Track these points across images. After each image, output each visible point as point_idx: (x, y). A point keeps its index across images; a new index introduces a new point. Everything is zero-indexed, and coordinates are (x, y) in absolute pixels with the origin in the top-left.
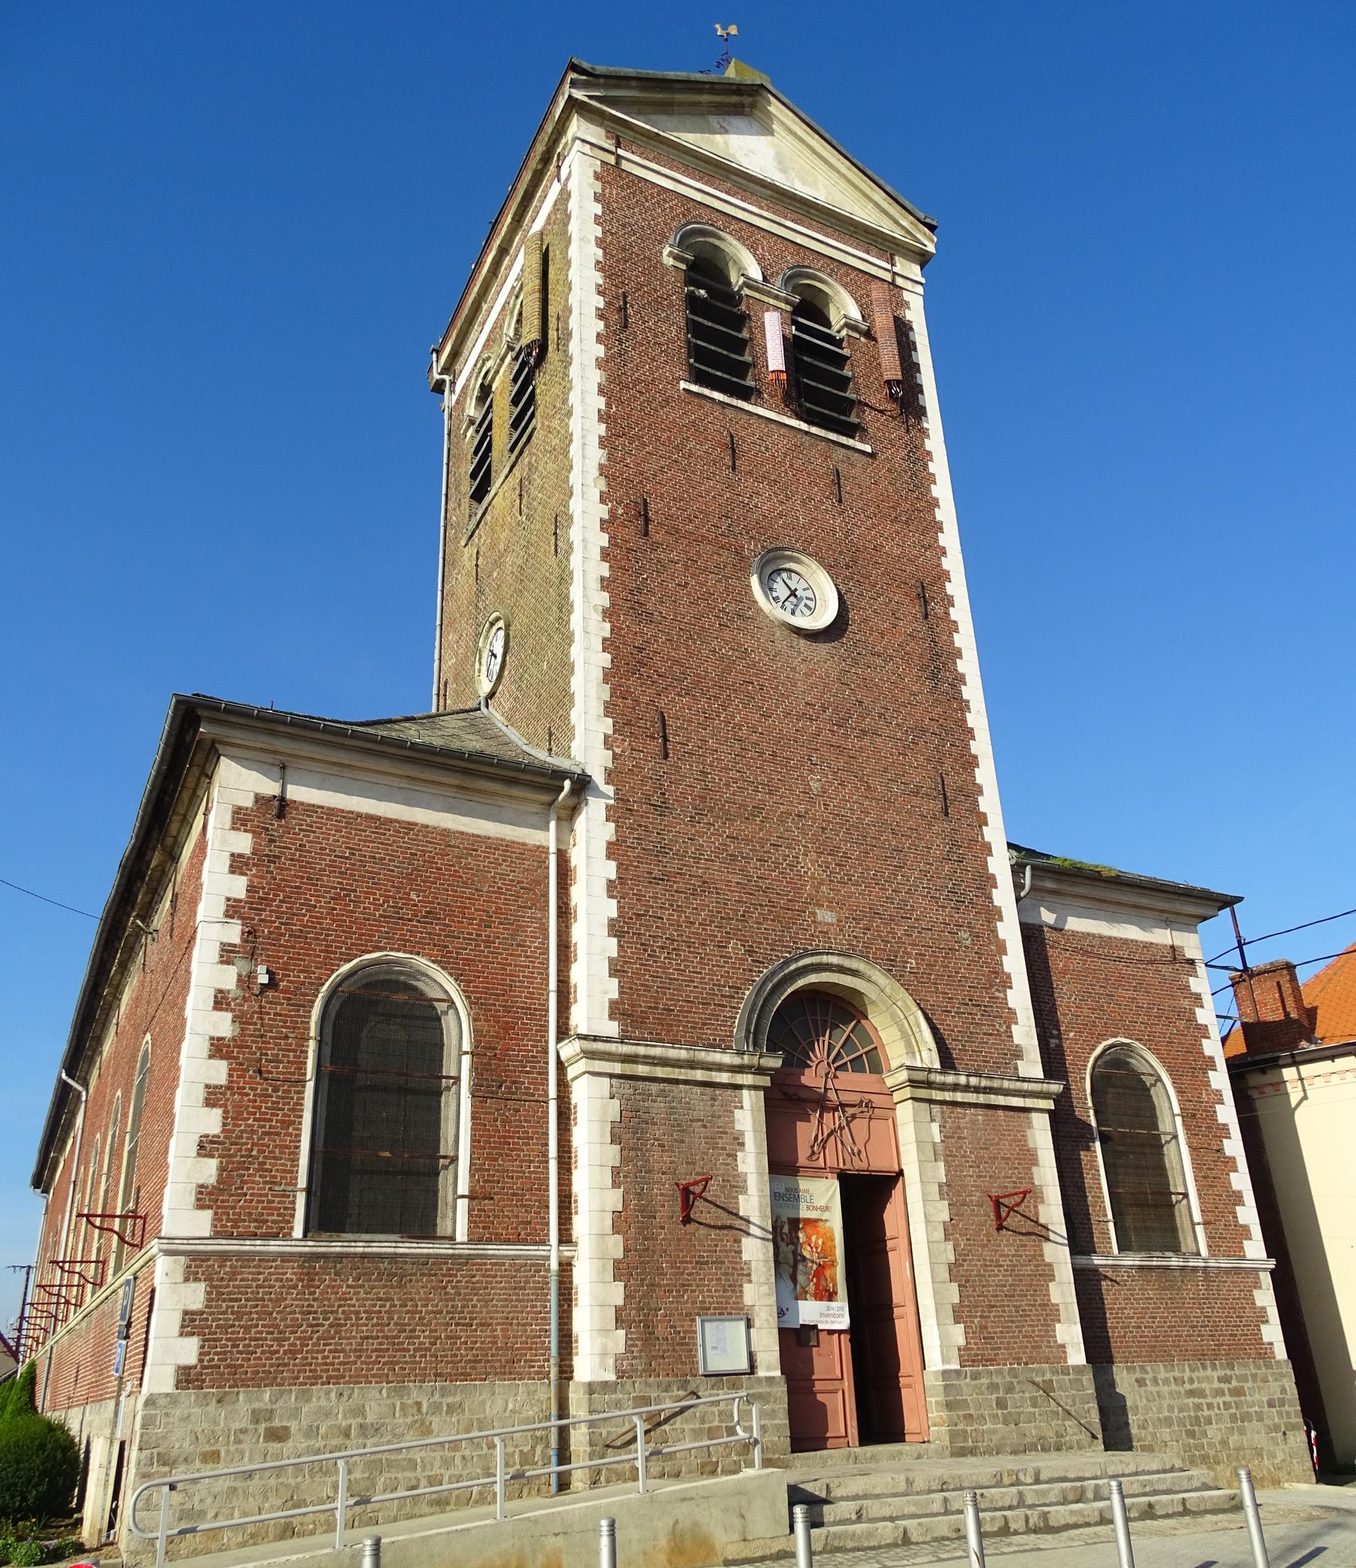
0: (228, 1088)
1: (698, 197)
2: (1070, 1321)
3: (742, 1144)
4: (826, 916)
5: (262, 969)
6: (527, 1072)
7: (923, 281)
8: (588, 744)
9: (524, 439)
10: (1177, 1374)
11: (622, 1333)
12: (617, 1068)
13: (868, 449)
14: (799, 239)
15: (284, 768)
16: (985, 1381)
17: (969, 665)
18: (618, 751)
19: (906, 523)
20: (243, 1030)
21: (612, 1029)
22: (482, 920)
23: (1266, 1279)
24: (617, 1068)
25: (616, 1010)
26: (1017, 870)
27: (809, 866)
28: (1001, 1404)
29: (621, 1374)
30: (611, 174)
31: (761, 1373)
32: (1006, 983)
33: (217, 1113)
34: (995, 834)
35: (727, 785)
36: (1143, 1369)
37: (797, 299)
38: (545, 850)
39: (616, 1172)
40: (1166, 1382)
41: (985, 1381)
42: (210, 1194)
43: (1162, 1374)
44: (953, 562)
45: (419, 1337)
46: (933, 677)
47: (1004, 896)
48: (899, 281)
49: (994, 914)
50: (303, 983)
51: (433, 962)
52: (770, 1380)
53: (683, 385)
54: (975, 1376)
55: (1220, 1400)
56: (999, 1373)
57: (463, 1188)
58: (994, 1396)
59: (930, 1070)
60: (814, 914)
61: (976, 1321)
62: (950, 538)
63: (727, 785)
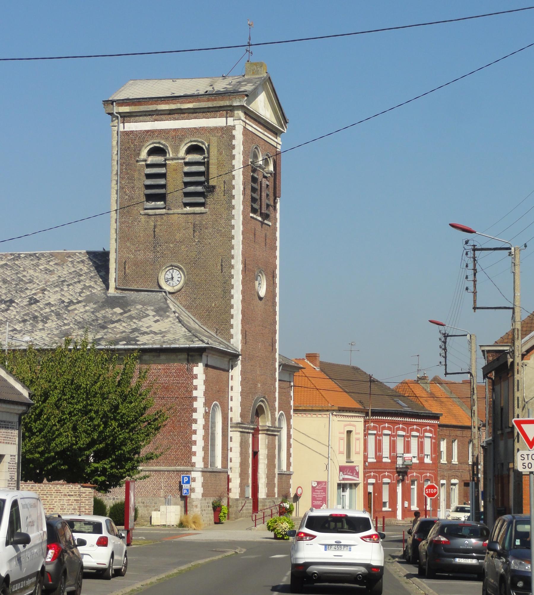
1: (254, 131)
4: (259, 385)
5: (207, 408)
7: (281, 143)
8: (237, 342)
12: (241, 430)
13: (270, 224)
14: (266, 139)
17: (277, 300)
21: (239, 420)
24: (241, 430)
25: (242, 416)
26: (279, 366)
27: (258, 373)
30: (246, 132)
34: (277, 356)
44: (278, 262)
53: (251, 215)
62: (278, 253)
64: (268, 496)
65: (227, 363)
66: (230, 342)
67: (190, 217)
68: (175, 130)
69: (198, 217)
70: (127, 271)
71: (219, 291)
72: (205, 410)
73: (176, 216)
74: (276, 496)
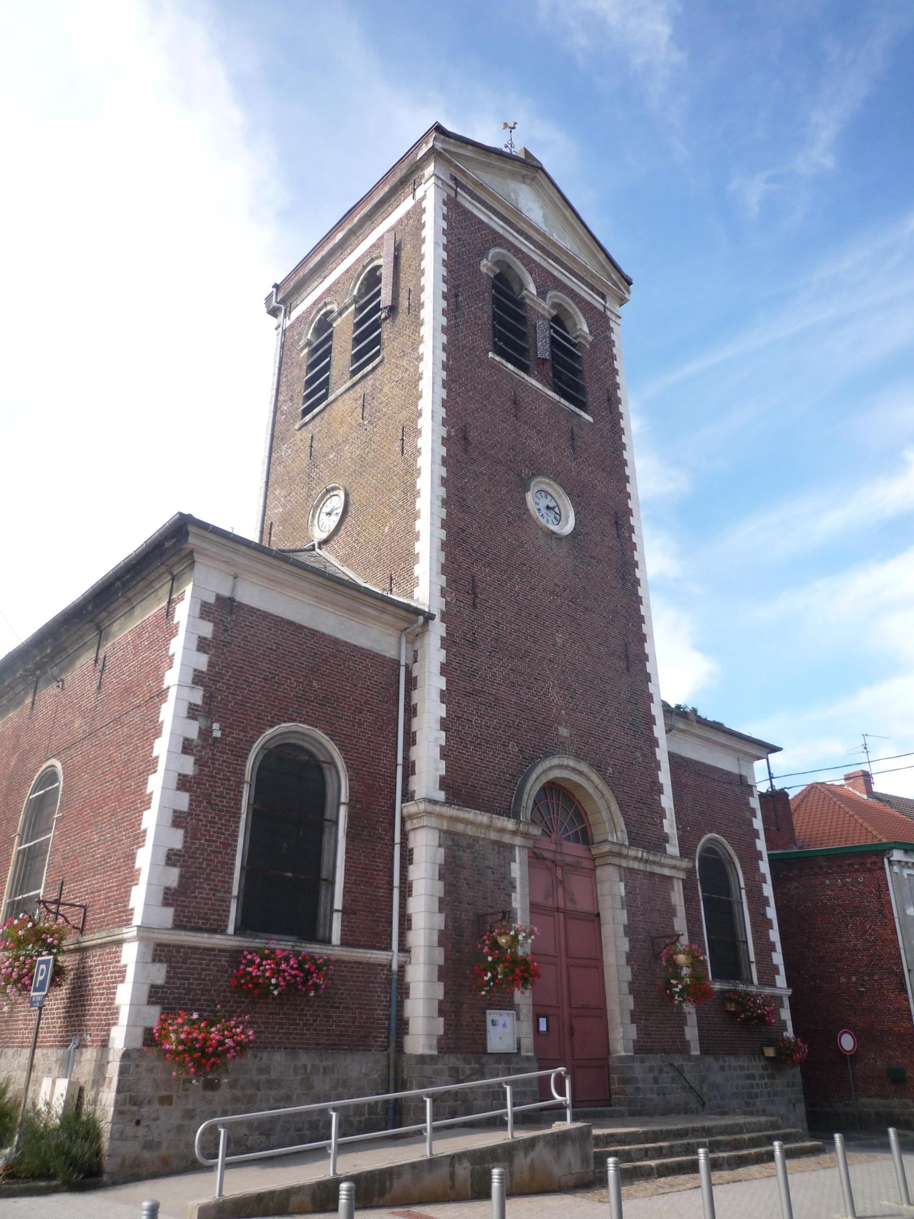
0: (189, 814)
2: (692, 1027)
3: (515, 887)
4: (564, 732)
5: (216, 726)
6: (381, 822)
9: (369, 368)
10: (741, 1063)
11: (442, 1019)
15: (236, 577)
16: (647, 1064)
18: (449, 599)
19: (609, 473)
20: (201, 770)
21: (441, 796)
22: (356, 708)
23: (786, 1003)
25: (444, 784)
27: (555, 696)
28: (656, 1081)
29: (440, 1049)
31: (523, 1054)
32: (660, 791)
33: (180, 833)
35: (510, 633)
36: (725, 1061)
37: (554, 313)
38: (398, 663)
39: (441, 900)
40: (735, 1068)
41: (647, 1064)
42: (173, 895)
43: (734, 1063)
45: (306, 1015)
46: (623, 578)
47: (659, 730)
48: (608, 313)
49: (654, 743)
50: (242, 740)
51: (326, 734)
52: (528, 1058)
53: (491, 355)
54: (643, 1062)
55: (763, 1082)
56: (654, 1061)
57: (338, 904)
58: (651, 1075)
59: (622, 845)
60: (557, 729)
61: (643, 1022)
63: (510, 633)
64: (641, 1048)
65: (393, 641)
66: (412, 598)
67: (358, 387)
68: (347, 271)
69: (369, 381)
70: (273, 538)
71: (397, 495)
72: (205, 733)
73: (340, 401)
74: (695, 1052)
